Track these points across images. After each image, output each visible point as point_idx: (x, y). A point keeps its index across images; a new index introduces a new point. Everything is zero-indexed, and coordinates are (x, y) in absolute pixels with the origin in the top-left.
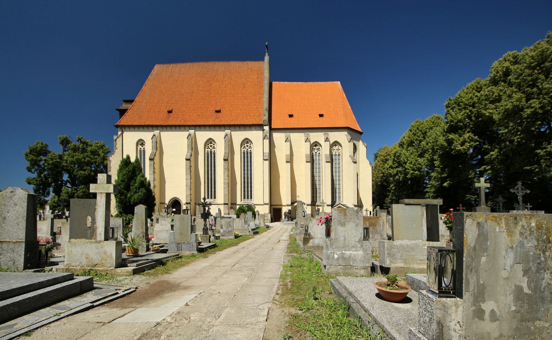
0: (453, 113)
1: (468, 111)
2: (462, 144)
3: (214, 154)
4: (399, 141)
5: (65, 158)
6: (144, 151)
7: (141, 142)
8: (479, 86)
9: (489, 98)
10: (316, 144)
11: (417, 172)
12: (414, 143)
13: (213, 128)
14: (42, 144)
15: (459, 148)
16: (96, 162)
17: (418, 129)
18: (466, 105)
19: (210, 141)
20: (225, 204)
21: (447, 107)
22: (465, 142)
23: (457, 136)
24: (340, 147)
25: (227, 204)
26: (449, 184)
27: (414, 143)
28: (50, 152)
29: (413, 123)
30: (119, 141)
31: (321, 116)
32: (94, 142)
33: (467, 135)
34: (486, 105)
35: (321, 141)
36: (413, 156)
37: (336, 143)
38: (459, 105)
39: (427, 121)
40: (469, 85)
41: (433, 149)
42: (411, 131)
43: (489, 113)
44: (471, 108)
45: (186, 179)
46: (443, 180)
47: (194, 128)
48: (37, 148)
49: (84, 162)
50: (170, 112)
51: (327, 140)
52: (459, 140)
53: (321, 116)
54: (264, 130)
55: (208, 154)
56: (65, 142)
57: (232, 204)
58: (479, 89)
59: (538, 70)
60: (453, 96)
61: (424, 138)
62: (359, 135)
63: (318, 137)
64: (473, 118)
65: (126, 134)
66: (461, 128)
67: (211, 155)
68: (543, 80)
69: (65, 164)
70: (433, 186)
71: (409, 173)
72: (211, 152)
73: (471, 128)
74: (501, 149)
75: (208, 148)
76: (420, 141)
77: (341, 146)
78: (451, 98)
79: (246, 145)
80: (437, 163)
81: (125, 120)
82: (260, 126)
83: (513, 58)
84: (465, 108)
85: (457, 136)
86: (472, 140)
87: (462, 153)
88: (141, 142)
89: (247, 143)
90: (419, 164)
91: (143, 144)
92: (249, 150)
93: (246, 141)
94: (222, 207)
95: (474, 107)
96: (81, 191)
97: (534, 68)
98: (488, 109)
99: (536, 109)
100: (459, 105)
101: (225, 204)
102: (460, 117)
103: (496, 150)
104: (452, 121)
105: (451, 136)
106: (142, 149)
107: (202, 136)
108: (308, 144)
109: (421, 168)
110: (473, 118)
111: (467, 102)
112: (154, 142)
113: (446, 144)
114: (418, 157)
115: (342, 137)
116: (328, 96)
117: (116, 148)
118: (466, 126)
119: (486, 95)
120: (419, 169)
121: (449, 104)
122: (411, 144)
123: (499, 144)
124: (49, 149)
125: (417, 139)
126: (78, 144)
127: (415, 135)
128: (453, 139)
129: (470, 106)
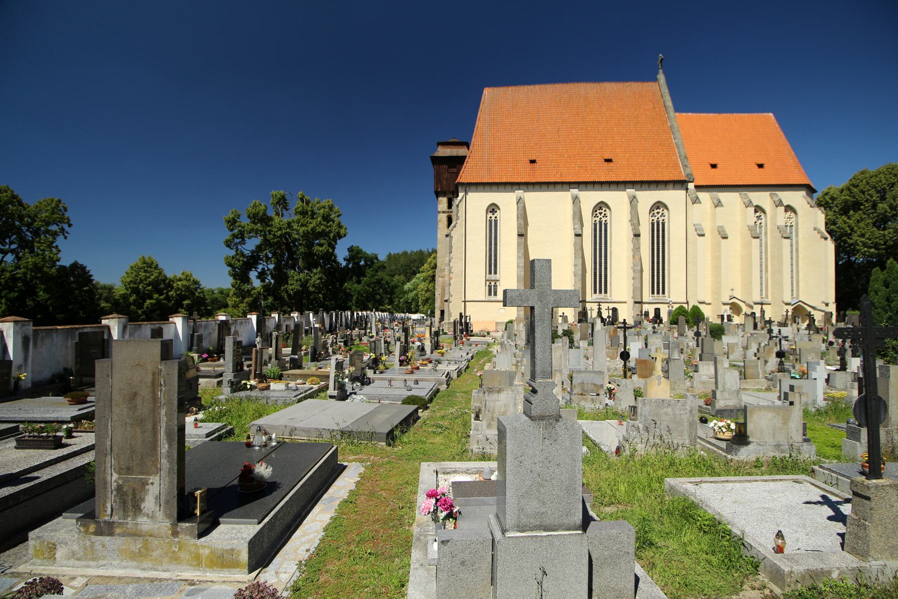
3: (606, 225)
6: (496, 221)
7: (493, 208)
10: (758, 209)
12: (862, 204)
16: (330, 232)
24: (793, 215)
31: (761, 166)
32: (321, 202)
47: (576, 186)
50: (533, 162)
53: (761, 166)
54: (687, 189)
55: (595, 225)
61: (883, 199)
63: (762, 198)
65: (471, 195)
67: (601, 227)
69: (297, 236)
72: (600, 222)
75: (596, 216)
79: (656, 211)
82: (681, 184)
88: (493, 208)
89: (658, 208)
91: (493, 211)
96: (317, 276)
106: (493, 218)
107: (590, 198)
108: (752, 210)
112: (520, 208)
115: (797, 199)
116: (751, 135)
117: (458, 218)
122: (856, 206)
127: (863, 192)
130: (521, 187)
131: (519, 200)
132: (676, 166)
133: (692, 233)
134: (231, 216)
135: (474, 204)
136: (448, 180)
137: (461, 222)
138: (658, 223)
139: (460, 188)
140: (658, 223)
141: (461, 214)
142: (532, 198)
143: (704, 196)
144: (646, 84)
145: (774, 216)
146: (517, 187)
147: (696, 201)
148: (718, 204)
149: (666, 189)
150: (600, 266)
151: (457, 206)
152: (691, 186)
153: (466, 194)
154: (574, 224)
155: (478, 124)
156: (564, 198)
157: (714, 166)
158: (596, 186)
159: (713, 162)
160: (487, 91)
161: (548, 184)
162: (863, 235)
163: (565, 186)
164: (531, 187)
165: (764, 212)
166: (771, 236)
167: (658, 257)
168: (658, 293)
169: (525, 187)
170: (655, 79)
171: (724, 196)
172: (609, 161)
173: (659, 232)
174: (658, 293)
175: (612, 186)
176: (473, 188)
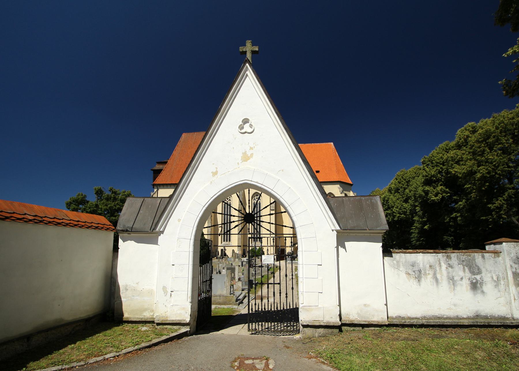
0: (427, 169)
1: (439, 168)
2: (436, 195)
4: (388, 187)
5: (100, 207)
8: (448, 148)
9: (455, 159)
11: (403, 215)
12: (399, 190)
14: (82, 195)
15: (434, 198)
17: (402, 177)
18: (438, 163)
20: (238, 246)
21: (423, 163)
22: (437, 193)
23: (432, 188)
25: (240, 246)
26: (429, 227)
27: (399, 190)
28: (88, 202)
29: (398, 173)
33: (439, 188)
34: (452, 165)
36: (398, 202)
38: (432, 163)
39: (410, 171)
40: (441, 146)
42: (397, 179)
43: (455, 171)
44: (441, 166)
46: (424, 224)
48: (79, 199)
49: (115, 209)
52: (434, 191)
56: (99, 193)
57: (244, 246)
58: (447, 151)
59: (484, 144)
60: (427, 156)
62: (349, 186)
64: (444, 174)
66: (435, 182)
68: (488, 152)
70: (417, 227)
71: (395, 216)
74: (467, 200)
76: (405, 189)
78: (426, 157)
80: (418, 209)
83: (472, 128)
84: (437, 166)
85: (432, 188)
86: (445, 192)
87: (436, 202)
89: (257, 196)
90: (405, 209)
94: (236, 250)
95: (444, 165)
97: (482, 142)
98: (454, 168)
99: (484, 174)
100: (432, 163)
101: (238, 246)
102: (433, 173)
103: (464, 201)
104: (426, 176)
105: (427, 188)
109: (406, 212)
111: (438, 161)
113: (423, 194)
114: (403, 202)
118: (438, 180)
119: (452, 157)
120: (405, 213)
121: (424, 161)
124: (87, 199)
125: (401, 187)
126: (110, 193)
128: (428, 191)
129: (441, 164)
134: (69, 200)
155: (174, 152)
160: (184, 135)
162: (397, 207)
176: (162, 187)
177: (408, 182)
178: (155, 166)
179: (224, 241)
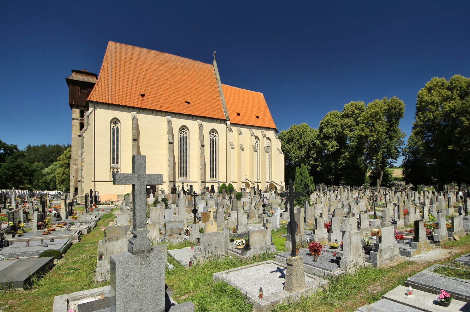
2: (332, 147)
3: (186, 138)
6: (117, 130)
7: (115, 121)
10: (257, 138)
13: (191, 118)
19: (184, 128)
27: (294, 139)
29: (292, 126)
30: (92, 117)
31: (258, 117)
35: (260, 136)
37: (268, 139)
41: (309, 146)
45: (169, 161)
47: (170, 114)
50: (143, 95)
51: (265, 136)
54: (227, 124)
61: (301, 138)
63: (258, 132)
64: (337, 134)
66: (331, 138)
72: (183, 137)
73: (335, 139)
75: (181, 133)
77: (271, 141)
79: (212, 134)
81: (94, 96)
82: (224, 121)
84: (332, 127)
88: (115, 121)
89: (213, 132)
91: (115, 123)
92: (214, 138)
93: (213, 131)
104: (327, 133)
105: (326, 142)
106: (115, 128)
107: (178, 123)
110: (337, 134)
112: (135, 123)
115: (271, 134)
116: (253, 101)
117: (88, 125)
118: (332, 137)
122: (292, 140)
123: (348, 150)
127: (294, 134)
128: (326, 143)
130: (135, 110)
131: (134, 118)
132: (221, 112)
133: (229, 147)
135: (101, 118)
136: (81, 97)
137: (91, 127)
138: (213, 140)
139: (90, 105)
140: (213, 140)
141: (91, 121)
142: (142, 118)
143: (234, 128)
144: (207, 65)
145: (263, 141)
146: (132, 109)
147: (231, 131)
148: (240, 133)
149: (217, 123)
150: (184, 161)
151: (88, 116)
152: (228, 123)
153: (95, 109)
154: (169, 136)
156: (162, 121)
157: (238, 114)
158: (181, 116)
159: (238, 112)
161: (153, 110)
162: (294, 153)
163: (163, 113)
164: (141, 111)
165: (259, 139)
166: (261, 151)
167: (213, 158)
168: (213, 177)
169: (138, 110)
170: (212, 63)
171: (243, 130)
172: (188, 103)
173: (213, 145)
174: (213, 177)
175: (190, 117)
176: (101, 106)
177: (301, 135)
178: (71, 75)
179: (181, 176)
